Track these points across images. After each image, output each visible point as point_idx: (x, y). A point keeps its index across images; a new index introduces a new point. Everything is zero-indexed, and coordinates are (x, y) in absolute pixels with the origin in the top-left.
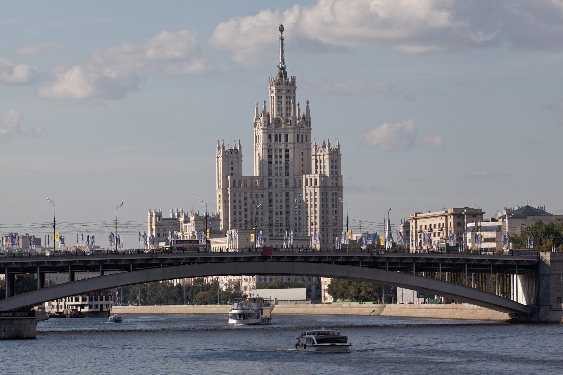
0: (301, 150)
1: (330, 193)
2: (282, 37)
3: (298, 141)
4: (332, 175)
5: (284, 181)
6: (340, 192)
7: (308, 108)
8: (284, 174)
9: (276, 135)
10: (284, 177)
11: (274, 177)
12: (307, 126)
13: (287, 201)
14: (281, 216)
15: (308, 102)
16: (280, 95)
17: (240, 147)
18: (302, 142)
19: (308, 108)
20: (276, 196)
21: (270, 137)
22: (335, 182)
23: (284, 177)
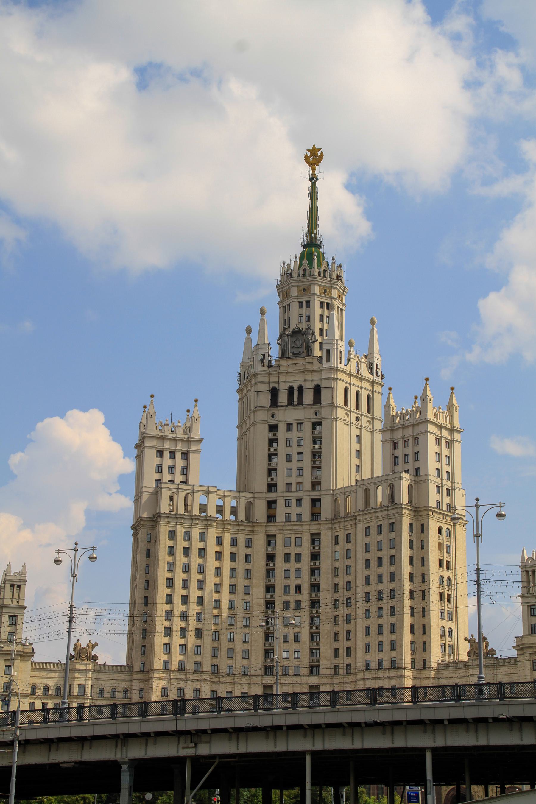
0: (353, 428)
1: (433, 525)
2: (313, 174)
3: (346, 404)
8: (307, 486)
9: (291, 390)
10: (308, 493)
11: (282, 495)
12: (372, 374)
13: (315, 556)
14: (298, 597)
16: (304, 299)
18: (357, 407)
21: (274, 393)
22: (447, 500)
23: (308, 493)
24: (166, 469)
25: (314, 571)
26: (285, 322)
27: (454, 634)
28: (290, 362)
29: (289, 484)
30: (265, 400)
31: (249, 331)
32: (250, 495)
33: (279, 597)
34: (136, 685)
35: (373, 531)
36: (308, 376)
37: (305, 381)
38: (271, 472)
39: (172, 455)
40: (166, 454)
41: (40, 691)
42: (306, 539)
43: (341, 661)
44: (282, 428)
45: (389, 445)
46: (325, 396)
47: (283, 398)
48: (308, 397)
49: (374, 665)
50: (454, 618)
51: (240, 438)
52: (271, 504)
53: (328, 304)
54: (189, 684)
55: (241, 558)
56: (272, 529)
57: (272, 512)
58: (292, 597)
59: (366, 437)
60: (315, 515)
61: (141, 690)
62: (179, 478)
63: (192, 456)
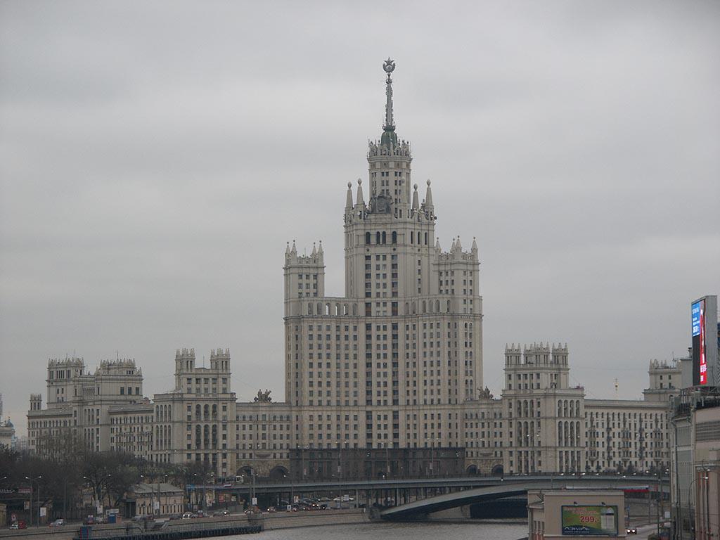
1: (461, 324)
2: (389, 79)
4: (465, 296)
5: (389, 305)
6: (477, 322)
7: (429, 190)
13: (395, 336)
14: (385, 361)
15: (428, 183)
16: (385, 171)
17: (321, 253)
18: (419, 243)
19: (429, 190)
20: (378, 328)
21: (368, 235)
24: (304, 286)
25: (395, 346)
26: (373, 184)
27: (474, 383)
28: (378, 216)
29: (378, 293)
30: (362, 241)
31: (350, 186)
32: (355, 300)
33: (374, 360)
34: (294, 415)
35: (428, 326)
36: (389, 226)
37: (387, 229)
38: (368, 285)
39: (308, 277)
40: (304, 276)
41: (241, 419)
42: (389, 327)
43: (411, 398)
44: (373, 258)
45: (437, 273)
46: (399, 239)
47: (373, 240)
48: (389, 240)
49: (429, 402)
50: (474, 374)
51: (346, 257)
52: (368, 305)
53: (400, 173)
54: (324, 412)
55: (351, 338)
56: (369, 321)
57: (368, 309)
58: (382, 361)
59: (424, 260)
60: (395, 313)
61: (297, 416)
62: (312, 290)
63: (319, 276)
